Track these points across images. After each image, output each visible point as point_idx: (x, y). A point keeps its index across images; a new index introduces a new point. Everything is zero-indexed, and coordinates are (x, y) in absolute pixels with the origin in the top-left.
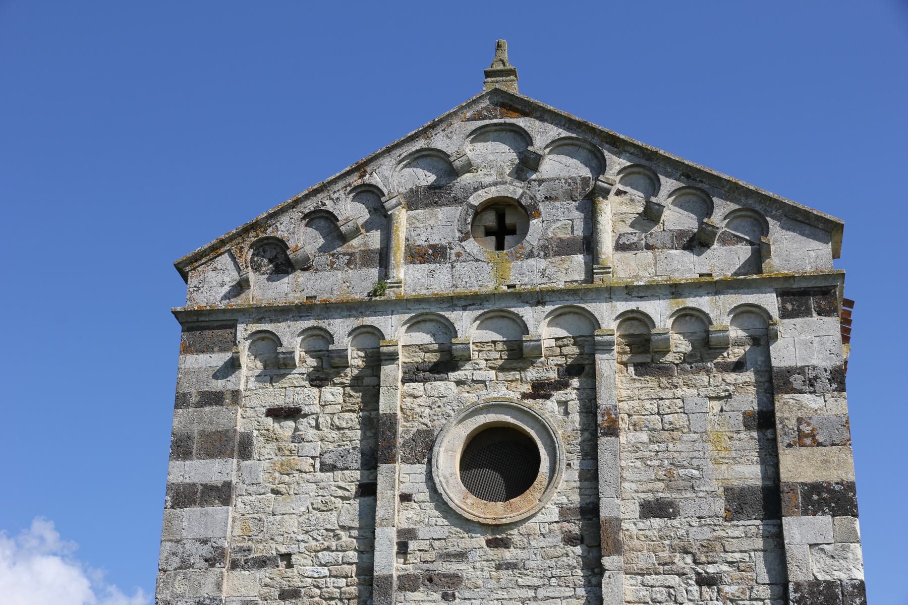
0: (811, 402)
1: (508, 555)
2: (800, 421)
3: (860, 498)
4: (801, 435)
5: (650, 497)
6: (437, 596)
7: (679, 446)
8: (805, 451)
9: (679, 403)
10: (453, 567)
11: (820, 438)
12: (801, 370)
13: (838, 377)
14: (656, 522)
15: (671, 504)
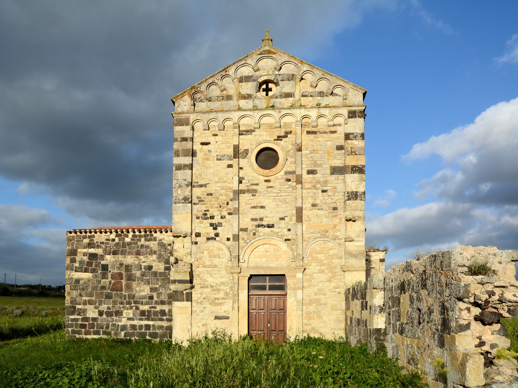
0: (355, 142)
1: (270, 184)
3: (366, 169)
4: (352, 152)
5: (310, 169)
6: (251, 195)
7: (318, 155)
10: (254, 187)
11: (357, 153)
12: (353, 134)
13: (363, 136)
15: (316, 171)
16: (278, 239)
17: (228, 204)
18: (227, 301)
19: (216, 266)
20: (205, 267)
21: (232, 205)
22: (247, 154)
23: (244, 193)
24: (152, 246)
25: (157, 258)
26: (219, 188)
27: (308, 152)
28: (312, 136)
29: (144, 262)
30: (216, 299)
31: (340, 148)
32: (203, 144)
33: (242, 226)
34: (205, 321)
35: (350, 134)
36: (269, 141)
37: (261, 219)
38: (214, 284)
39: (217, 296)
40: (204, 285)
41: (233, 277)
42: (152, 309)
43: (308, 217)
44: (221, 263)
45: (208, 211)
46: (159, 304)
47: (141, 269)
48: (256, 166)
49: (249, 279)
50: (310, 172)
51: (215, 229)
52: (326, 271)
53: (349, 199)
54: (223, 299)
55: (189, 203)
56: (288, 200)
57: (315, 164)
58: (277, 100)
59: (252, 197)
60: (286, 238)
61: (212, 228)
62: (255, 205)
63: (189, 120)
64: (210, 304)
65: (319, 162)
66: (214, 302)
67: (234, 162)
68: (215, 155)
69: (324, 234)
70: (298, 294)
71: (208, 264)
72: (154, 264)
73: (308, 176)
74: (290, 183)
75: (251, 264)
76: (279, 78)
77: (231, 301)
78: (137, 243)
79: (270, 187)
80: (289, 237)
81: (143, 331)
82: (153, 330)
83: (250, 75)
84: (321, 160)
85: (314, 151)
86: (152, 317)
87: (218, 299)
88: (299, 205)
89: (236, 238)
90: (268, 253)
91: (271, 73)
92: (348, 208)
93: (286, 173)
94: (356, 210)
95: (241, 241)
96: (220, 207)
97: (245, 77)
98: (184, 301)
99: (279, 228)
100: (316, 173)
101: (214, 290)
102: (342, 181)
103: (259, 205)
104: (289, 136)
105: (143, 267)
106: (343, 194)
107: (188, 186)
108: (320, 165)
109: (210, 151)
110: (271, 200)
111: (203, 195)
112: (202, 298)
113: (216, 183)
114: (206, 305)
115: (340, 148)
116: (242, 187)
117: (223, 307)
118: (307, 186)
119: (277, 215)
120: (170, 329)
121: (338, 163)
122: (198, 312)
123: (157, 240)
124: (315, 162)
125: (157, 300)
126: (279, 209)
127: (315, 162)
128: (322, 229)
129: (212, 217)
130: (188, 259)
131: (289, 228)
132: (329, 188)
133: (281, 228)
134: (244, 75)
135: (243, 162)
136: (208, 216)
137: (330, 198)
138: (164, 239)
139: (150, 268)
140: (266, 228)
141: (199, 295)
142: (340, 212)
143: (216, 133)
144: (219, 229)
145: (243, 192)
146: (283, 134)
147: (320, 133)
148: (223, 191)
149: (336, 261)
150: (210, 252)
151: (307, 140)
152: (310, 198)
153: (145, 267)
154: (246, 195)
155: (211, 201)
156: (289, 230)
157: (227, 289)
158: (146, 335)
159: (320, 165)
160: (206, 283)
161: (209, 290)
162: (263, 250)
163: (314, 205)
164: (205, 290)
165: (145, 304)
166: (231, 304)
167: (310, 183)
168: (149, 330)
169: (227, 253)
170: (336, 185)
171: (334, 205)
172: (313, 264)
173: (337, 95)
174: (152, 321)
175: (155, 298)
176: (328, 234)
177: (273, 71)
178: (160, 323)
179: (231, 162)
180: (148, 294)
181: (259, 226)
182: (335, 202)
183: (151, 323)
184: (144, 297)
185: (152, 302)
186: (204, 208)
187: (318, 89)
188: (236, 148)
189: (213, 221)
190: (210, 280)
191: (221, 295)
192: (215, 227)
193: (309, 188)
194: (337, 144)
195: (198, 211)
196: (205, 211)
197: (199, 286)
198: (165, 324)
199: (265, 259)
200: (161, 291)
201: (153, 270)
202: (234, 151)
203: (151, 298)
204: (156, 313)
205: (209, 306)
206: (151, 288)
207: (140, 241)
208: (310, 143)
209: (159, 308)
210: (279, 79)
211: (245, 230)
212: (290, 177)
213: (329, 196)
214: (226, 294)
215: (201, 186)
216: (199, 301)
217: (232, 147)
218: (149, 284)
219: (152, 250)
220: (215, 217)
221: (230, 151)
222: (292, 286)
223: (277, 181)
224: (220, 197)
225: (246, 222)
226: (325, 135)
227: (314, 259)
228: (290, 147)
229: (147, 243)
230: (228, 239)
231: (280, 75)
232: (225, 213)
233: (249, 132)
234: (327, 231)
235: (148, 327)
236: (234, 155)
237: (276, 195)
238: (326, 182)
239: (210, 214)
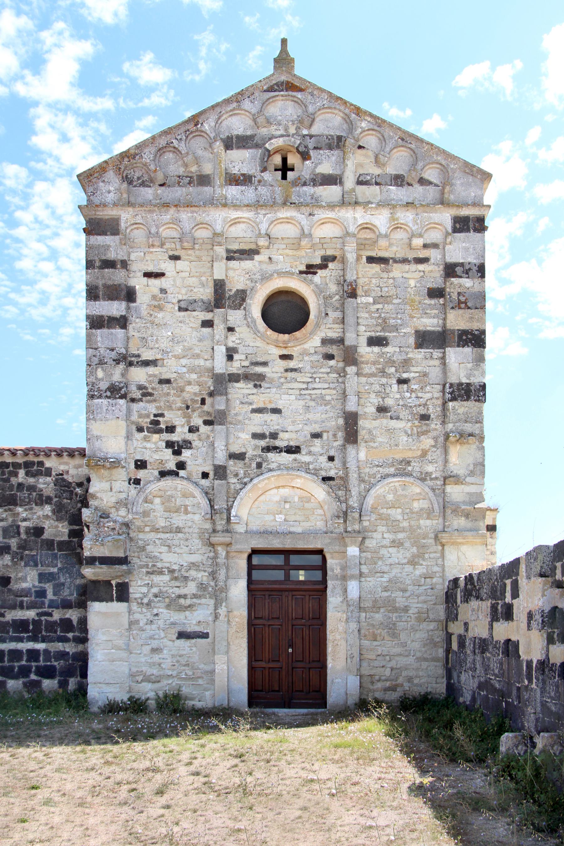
0: (467, 282)
1: (292, 364)
2: (459, 294)
4: (460, 302)
5: (373, 334)
6: (251, 385)
7: (391, 306)
8: (461, 312)
9: (391, 281)
10: (259, 369)
11: (469, 304)
12: (462, 265)
14: (376, 349)
15: (385, 339)
16: (308, 476)
17: (203, 402)
18: (203, 601)
19: (179, 530)
21: (213, 405)
22: (244, 300)
23: (237, 381)
24: (41, 486)
25: (53, 512)
26: (185, 370)
27: (371, 300)
28: (376, 268)
29: (25, 520)
30: (179, 596)
31: (436, 293)
32: (148, 275)
33: (236, 449)
35: (456, 265)
36: (289, 274)
37: (274, 436)
38: (176, 567)
39: (183, 591)
41: (216, 552)
42: (43, 618)
43: (370, 432)
45: (162, 415)
46: (57, 608)
47: (19, 533)
48: (261, 324)
49: (250, 558)
50: (373, 342)
51: (177, 453)
52: (407, 544)
53: (454, 399)
54: (195, 596)
55: (121, 397)
56: (328, 398)
57: (385, 324)
58: (305, 188)
59: (255, 391)
60: (324, 474)
61: (170, 451)
62: (261, 405)
63: (118, 224)
64: (168, 607)
65: (392, 322)
67: (217, 315)
68: (175, 301)
69: (402, 468)
70: (349, 588)
72: (46, 524)
73: (369, 349)
74: (332, 363)
75: (254, 527)
76: (311, 144)
77: (212, 602)
79: (292, 370)
80: (332, 473)
82: (45, 660)
83: (249, 133)
84: (396, 318)
85: (382, 299)
86: (44, 633)
87: (185, 597)
88: (351, 406)
89: (221, 472)
90: (287, 506)
91: (292, 130)
92: (452, 416)
93: (325, 342)
94: (466, 422)
95: (233, 480)
96: (188, 407)
97: (238, 137)
99: (310, 453)
100: (387, 345)
101: (176, 579)
102: (437, 363)
103: (270, 406)
104: (331, 265)
105: (22, 530)
106: (439, 387)
107: (117, 361)
108: (396, 328)
109: (163, 291)
110: (293, 397)
111: (150, 382)
113: (178, 357)
115: (436, 293)
116: (235, 367)
117: (195, 613)
118: (367, 369)
119: (306, 428)
120: (82, 660)
121: (430, 323)
123: (54, 473)
124: (384, 320)
125: (55, 598)
126: (310, 416)
127: (384, 320)
128: (399, 457)
129: (171, 429)
130: (121, 515)
131: (332, 453)
132: (412, 375)
133: (315, 454)
134: (235, 133)
135: (235, 317)
136: (163, 426)
137: (414, 395)
138: (67, 472)
139: (38, 531)
140: (284, 454)
141: (145, 590)
142: (435, 425)
143: (176, 253)
144: (186, 454)
145: (234, 378)
146: (318, 261)
147: (395, 261)
148: (194, 376)
149: (425, 523)
150: (167, 499)
151: (366, 275)
152: (373, 396)
153: (28, 529)
154: (241, 385)
155: (168, 394)
156: (331, 459)
157: (202, 576)
158: (30, 671)
159: (396, 328)
160: (159, 565)
161: (166, 578)
162: (277, 498)
163: (382, 410)
164: (157, 579)
165: (28, 608)
166: (212, 607)
167: (374, 363)
169: (204, 503)
170: (427, 370)
171: (422, 411)
172: (381, 529)
173: (430, 183)
174: (43, 641)
175: (50, 595)
176: (410, 468)
177: (298, 128)
178: (60, 646)
179: (208, 316)
180: (34, 586)
181: (268, 449)
182: (425, 405)
183: (41, 646)
184: (26, 593)
185: (43, 603)
186: (152, 409)
187: (391, 170)
188: (219, 286)
189: (174, 437)
190: (169, 559)
191: (191, 588)
192: (176, 448)
193: (372, 375)
194: (430, 285)
195: (140, 416)
196: (155, 416)
198: (70, 648)
199: (283, 517)
200: (62, 580)
201: (46, 536)
202: (216, 291)
203: (41, 593)
204: (51, 626)
206: (40, 575)
207: (16, 475)
208: (374, 281)
209: (57, 615)
210: (311, 146)
211: (240, 457)
212: (333, 350)
213: (412, 391)
214: (202, 587)
215: (147, 363)
216: (146, 601)
217: (211, 284)
218: (36, 565)
219: (41, 495)
220: (178, 429)
221: (206, 293)
222: (338, 571)
223: (306, 358)
224: (188, 388)
225: (242, 440)
226: (406, 267)
227: (381, 517)
228: (333, 288)
229: (31, 480)
230: (205, 475)
231: (311, 136)
232: (197, 421)
233: (248, 254)
234: (409, 463)
235: (33, 654)
236: (216, 300)
237: (305, 386)
238: (406, 363)
239: (166, 422)
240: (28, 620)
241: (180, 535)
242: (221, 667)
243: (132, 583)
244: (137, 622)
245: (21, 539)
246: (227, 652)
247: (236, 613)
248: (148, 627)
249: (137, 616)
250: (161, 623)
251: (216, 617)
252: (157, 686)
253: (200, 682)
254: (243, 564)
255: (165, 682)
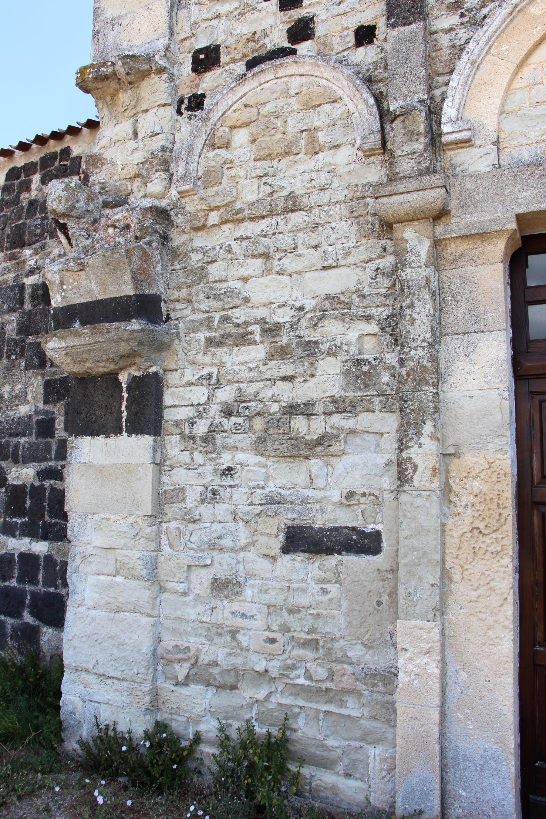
18: (364, 420)
19: (293, 205)
20: (235, 218)
30: (292, 410)
34: (226, 558)
38: (283, 316)
39: (301, 392)
40: (229, 328)
42: (47, 483)
44: (322, 178)
54: (338, 406)
64: (260, 445)
66: (285, 433)
71: (252, 197)
77: (390, 422)
78: (16, 201)
81: (14, 583)
87: (306, 409)
98: (118, 431)
101: (282, 353)
105: (28, 292)
112: (214, 410)
114: (241, 456)
117: (340, 464)
122: (191, 498)
141: (199, 394)
157: (358, 336)
160: (240, 315)
161: (257, 352)
165: (25, 462)
166: (390, 443)
168: (34, 581)
174: (45, 538)
184: (20, 427)
185: (48, 446)
190: (268, 294)
191: (327, 379)
197: (201, 336)
205: (252, 459)
214: (360, 372)
216: (201, 428)
240: (24, 485)
241: (297, 218)
242: (416, 665)
243: (172, 378)
244: (179, 493)
245: (24, 313)
246: (441, 609)
247: (471, 460)
248: (206, 510)
249: (180, 477)
250: (240, 496)
251: (403, 473)
252: (226, 700)
253: (352, 708)
254: (489, 278)
255: (249, 693)
